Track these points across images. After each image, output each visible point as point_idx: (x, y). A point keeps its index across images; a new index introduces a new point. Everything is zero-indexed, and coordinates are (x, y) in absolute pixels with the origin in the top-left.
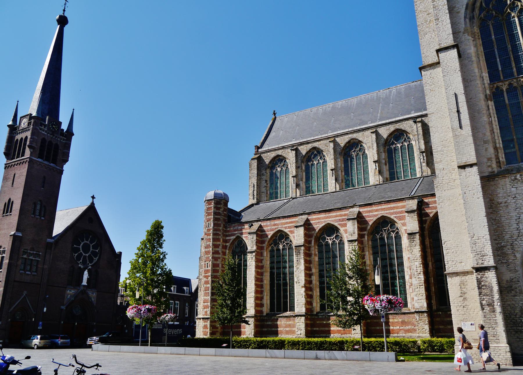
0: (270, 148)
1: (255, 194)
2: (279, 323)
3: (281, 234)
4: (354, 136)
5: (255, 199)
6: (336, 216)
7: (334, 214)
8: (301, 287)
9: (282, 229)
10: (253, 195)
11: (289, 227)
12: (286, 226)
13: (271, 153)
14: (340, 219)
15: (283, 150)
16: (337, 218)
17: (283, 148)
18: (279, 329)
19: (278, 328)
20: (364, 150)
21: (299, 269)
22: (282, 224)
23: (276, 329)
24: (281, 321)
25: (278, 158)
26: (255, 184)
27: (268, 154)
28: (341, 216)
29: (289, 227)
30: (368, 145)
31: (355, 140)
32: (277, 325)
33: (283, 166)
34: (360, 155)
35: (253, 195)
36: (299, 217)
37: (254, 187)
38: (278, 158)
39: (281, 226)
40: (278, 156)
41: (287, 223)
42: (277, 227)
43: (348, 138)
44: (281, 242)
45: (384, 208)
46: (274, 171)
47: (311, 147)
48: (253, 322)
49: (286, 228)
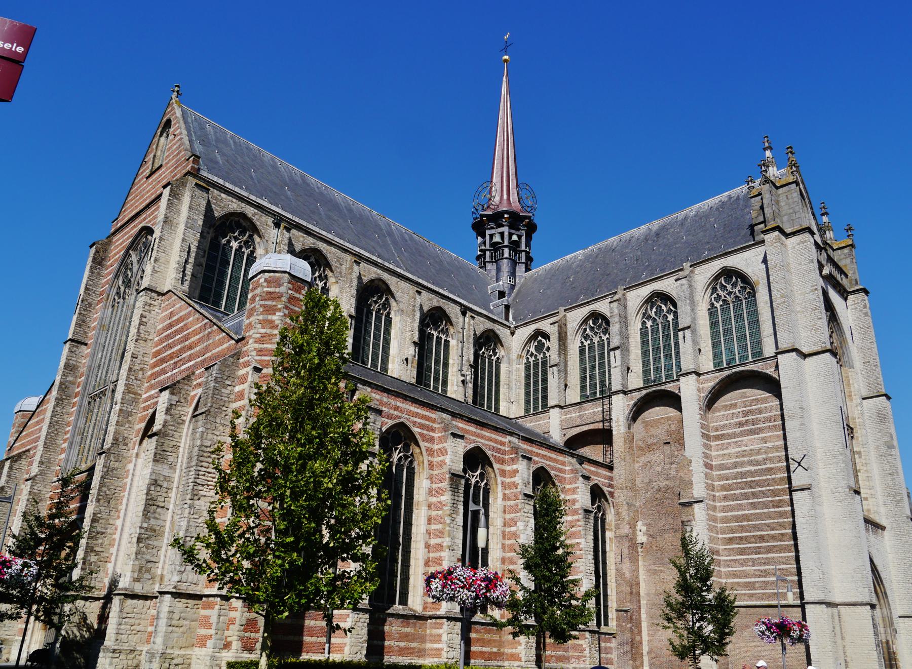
0: (227, 185)
1: (189, 271)
2: (386, 628)
3: (397, 431)
4: (386, 276)
5: (187, 284)
6: (490, 439)
7: (488, 434)
8: (456, 560)
9: (408, 424)
10: (184, 272)
11: (421, 426)
12: (415, 419)
13: (230, 198)
14: (494, 447)
15: (256, 211)
16: (491, 443)
17: (259, 207)
18: (387, 643)
19: (385, 640)
20: (390, 309)
21: (455, 523)
22: (409, 413)
23: (380, 643)
24: (391, 623)
25: (237, 219)
26: (194, 249)
27: (223, 195)
28: (496, 441)
29: (421, 426)
30: (402, 306)
31: (381, 283)
32: (383, 632)
33: (246, 242)
34: (382, 314)
35: (184, 272)
36: (438, 413)
37: (189, 252)
38: (237, 219)
39: (407, 417)
40: (243, 216)
41: (417, 415)
42: (400, 414)
43: (375, 273)
44: (396, 449)
45: (545, 456)
46: (224, 241)
47: (312, 246)
48: (366, 624)
49: (414, 423)
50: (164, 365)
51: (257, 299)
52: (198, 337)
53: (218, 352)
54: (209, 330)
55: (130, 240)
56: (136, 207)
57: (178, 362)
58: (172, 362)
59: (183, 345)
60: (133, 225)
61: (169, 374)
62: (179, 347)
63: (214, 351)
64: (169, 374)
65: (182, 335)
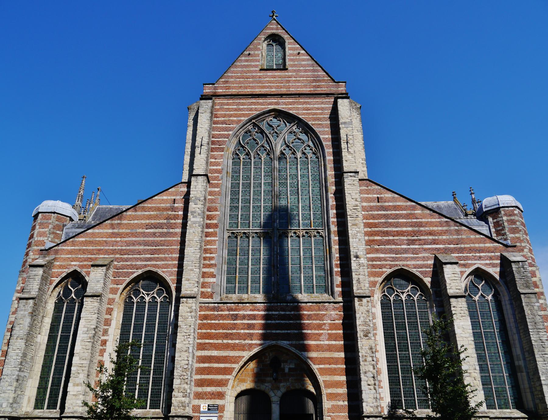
50: (391, 238)
51: (518, 223)
52: (440, 228)
53: (479, 247)
54: (457, 228)
55: (258, 112)
56: (253, 87)
57: (414, 240)
58: (405, 238)
59: (416, 229)
60: (253, 100)
61: (403, 247)
62: (410, 229)
63: (472, 245)
64: (403, 247)
65: (410, 220)
